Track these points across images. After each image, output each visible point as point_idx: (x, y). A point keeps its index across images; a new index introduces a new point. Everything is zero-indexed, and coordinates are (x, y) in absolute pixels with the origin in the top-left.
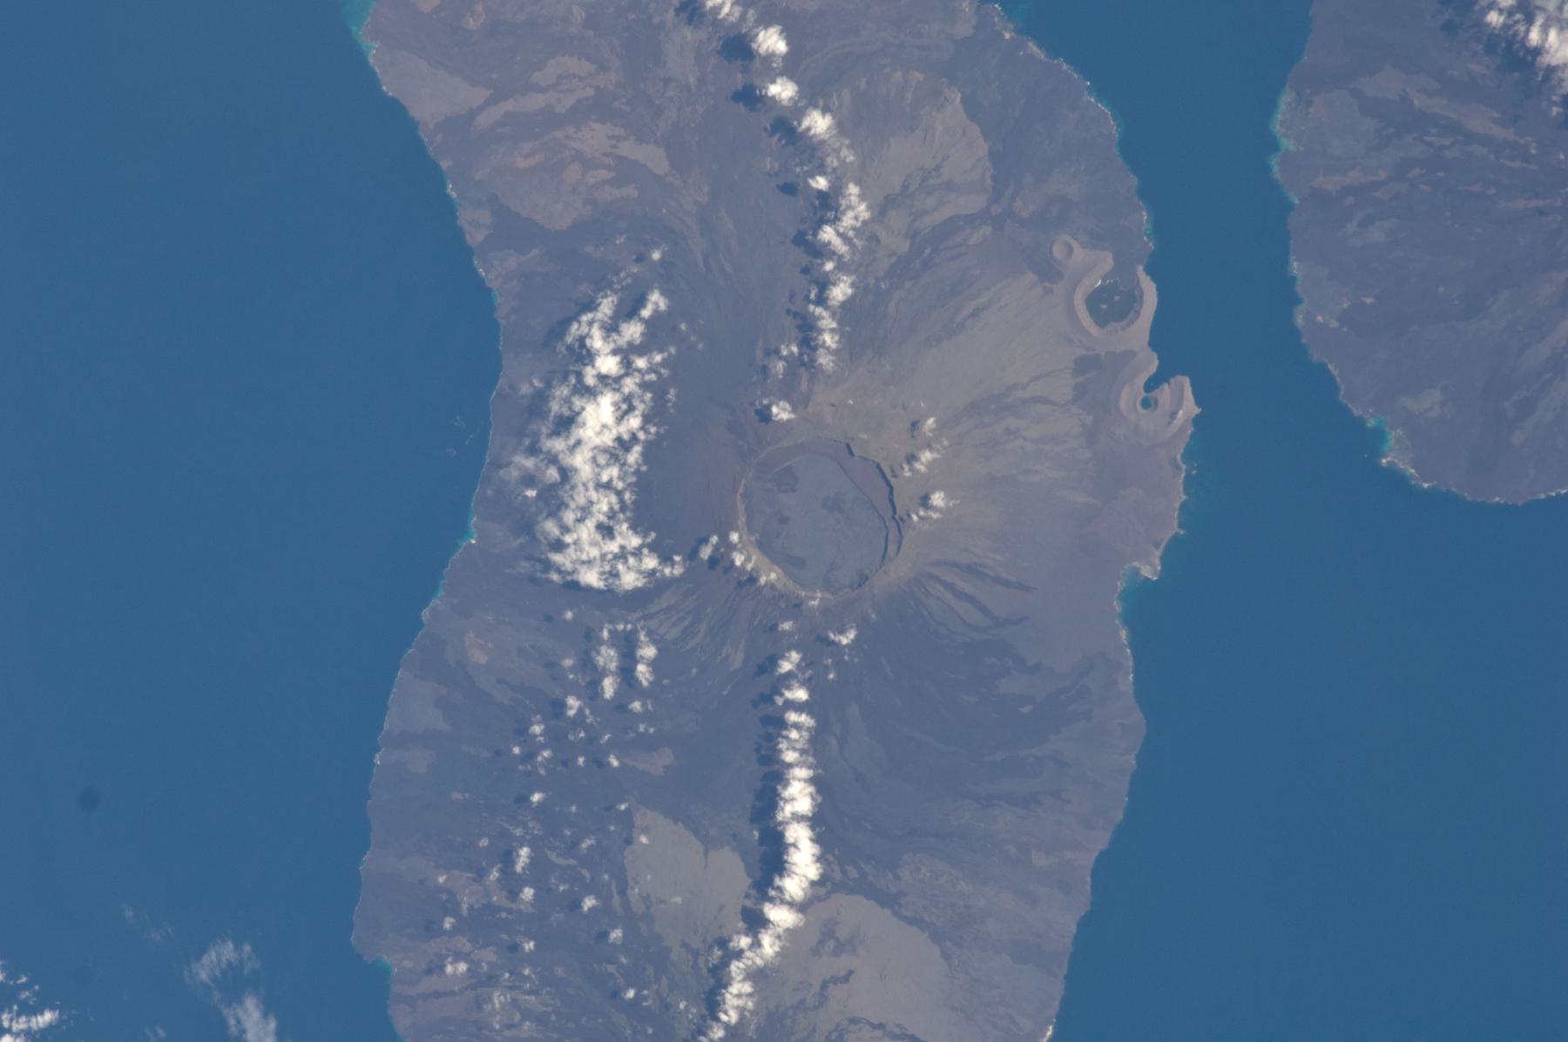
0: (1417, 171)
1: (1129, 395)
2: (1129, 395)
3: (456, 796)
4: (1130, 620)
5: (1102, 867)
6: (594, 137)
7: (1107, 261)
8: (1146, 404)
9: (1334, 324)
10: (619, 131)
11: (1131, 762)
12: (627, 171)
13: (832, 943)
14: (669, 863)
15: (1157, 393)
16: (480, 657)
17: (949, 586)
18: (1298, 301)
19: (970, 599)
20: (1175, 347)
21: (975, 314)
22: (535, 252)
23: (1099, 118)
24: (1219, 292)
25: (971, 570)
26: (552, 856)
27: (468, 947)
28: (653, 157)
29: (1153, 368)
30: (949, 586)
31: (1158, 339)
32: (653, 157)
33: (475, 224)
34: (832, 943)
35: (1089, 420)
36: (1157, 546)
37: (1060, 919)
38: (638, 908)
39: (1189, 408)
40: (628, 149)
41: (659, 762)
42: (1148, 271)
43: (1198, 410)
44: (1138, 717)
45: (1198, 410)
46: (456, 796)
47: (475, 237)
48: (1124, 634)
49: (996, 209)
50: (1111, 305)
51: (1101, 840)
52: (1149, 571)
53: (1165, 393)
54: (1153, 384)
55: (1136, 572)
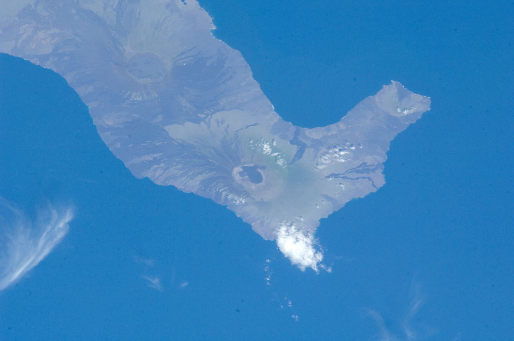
3: (130, 146)
4: (219, 38)
5: (255, 77)
6: (41, 34)
11: (242, 58)
13: (220, 123)
16: (110, 123)
17: (182, 59)
22: (51, 58)
25: (182, 53)
26: (157, 144)
27: (157, 166)
30: (182, 59)
33: (36, 61)
34: (220, 123)
37: (256, 89)
38: (181, 142)
40: (49, 32)
41: (160, 118)
44: (237, 51)
46: (130, 146)
47: (38, 63)
48: (220, 41)
51: (251, 74)
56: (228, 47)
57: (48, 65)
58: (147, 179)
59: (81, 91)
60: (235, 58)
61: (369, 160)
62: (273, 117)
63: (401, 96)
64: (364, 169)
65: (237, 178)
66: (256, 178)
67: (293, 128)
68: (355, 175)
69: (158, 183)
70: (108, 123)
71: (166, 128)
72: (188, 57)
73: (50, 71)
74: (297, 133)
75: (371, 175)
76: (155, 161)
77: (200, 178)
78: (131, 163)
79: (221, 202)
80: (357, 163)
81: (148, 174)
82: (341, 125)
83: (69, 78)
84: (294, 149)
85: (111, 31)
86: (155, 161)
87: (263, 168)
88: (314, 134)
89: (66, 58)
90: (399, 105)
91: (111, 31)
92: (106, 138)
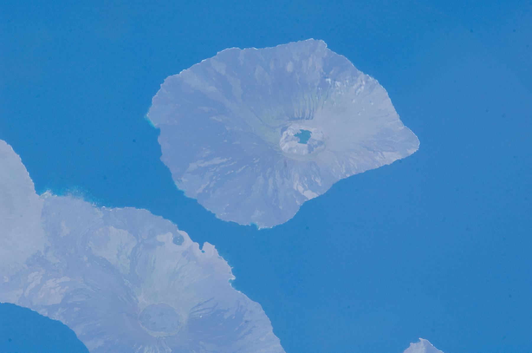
0: (214, 178)
1: (198, 252)
4: (238, 289)
6: (50, 283)
7: (171, 234)
8: (203, 252)
9: (225, 213)
10: (54, 279)
11: (263, 312)
15: (203, 249)
17: (198, 311)
18: (214, 214)
19: (204, 309)
20: (199, 238)
21: (154, 263)
22: (60, 309)
23: (143, 213)
24: (198, 223)
25: (199, 305)
29: (198, 245)
30: (198, 311)
31: (194, 239)
33: (44, 312)
35: (195, 262)
36: (230, 273)
39: (213, 247)
42: (180, 229)
43: (214, 246)
44: (257, 304)
45: (214, 246)
47: (46, 314)
48: (239, 292)
49: (140, 241)
50: (178, 241)
52: (233, 278)
53: (204, 248)
54: (201, 248)
55: (231, 280)
56: (248, 299)
57: (56, 316)
60: (255, 311)
72: (204, 309)
85: (125, 280)
89: (76, 309)
91: (125, 280)
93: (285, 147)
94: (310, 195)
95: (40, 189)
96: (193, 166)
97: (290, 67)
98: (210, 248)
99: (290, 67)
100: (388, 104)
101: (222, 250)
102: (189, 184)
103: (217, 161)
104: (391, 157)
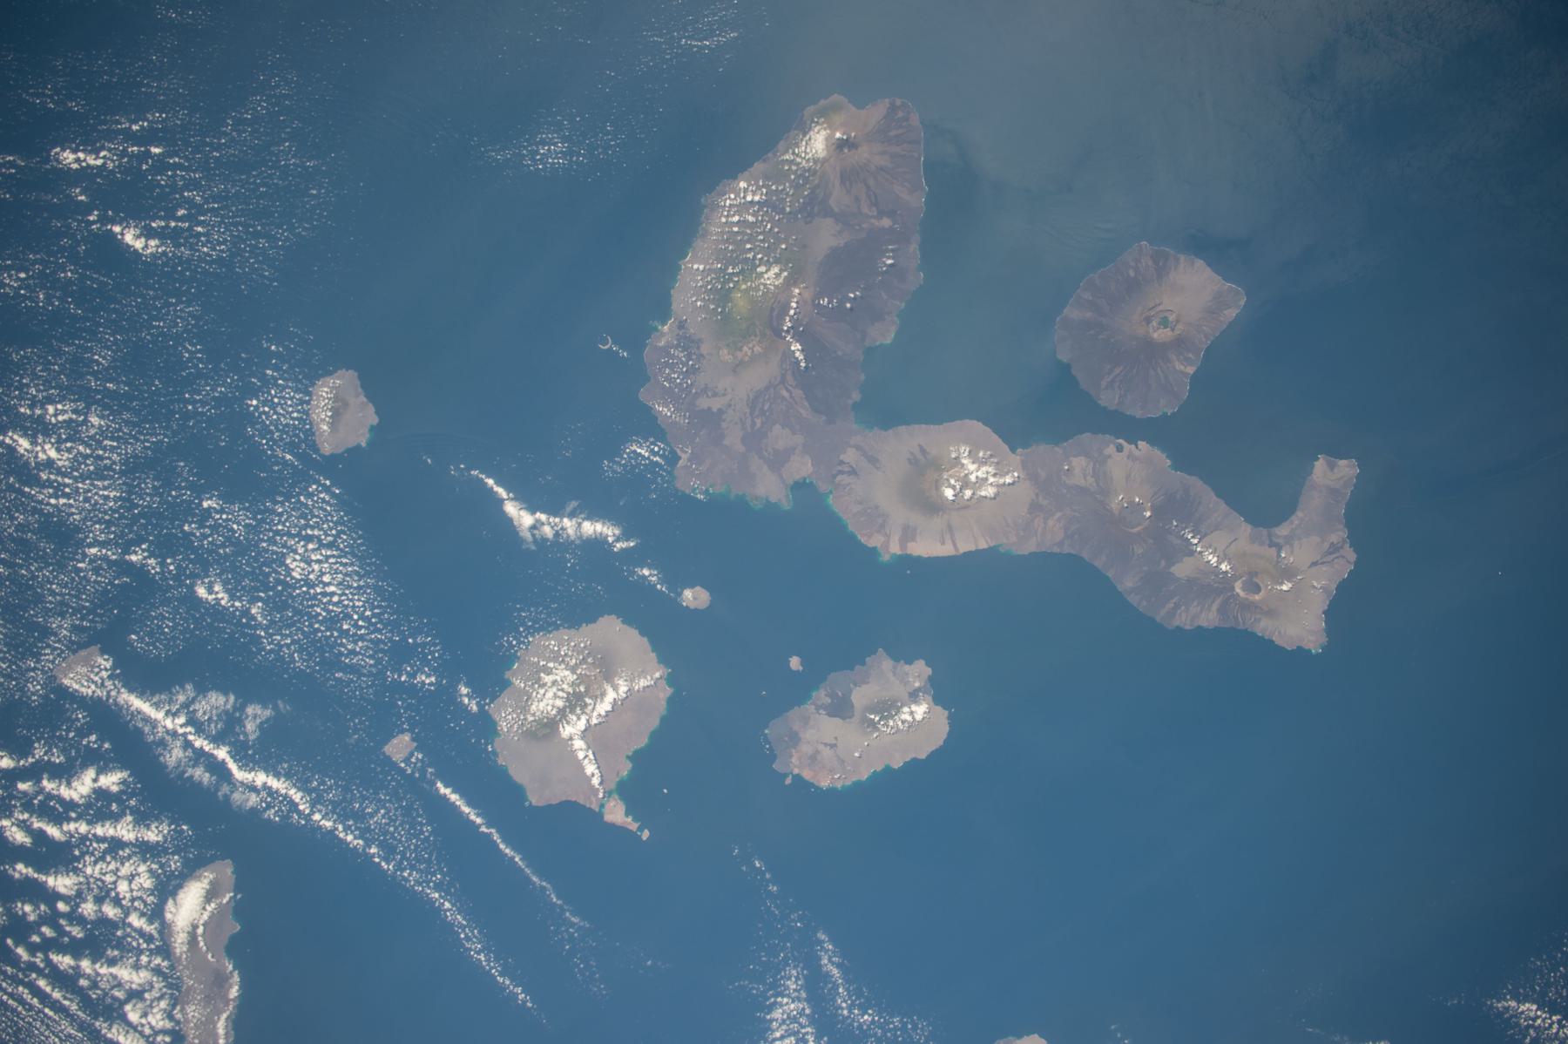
1: (1136, 452)
2: (1136, 452)
6: (1051, 522)
12: (1059, 520)
14: (1182, 569)
23: (1086, 436)
28: (1058, 514)
32: (1058, 514)
33: (1056, 550)
37: (1223, 506)
41: (1163, 563)
50: (1120, 449)
57: (1066, 549)
58: (1178, 628)
59: (1099, 563)
60: (1195, 483)
61: (1334, 538)
62: (1246, 529)
63: (1332, 466)
64: (1334, 548)
65: (1242, 594)
66: (1258, 589)
67: (1264, 532)
68: (1329, 558)
69: (1188, 627)
70: (1128, 583)
71: (1172, 569)
73: (1069, 555)
74: (1270, 535)
75: (1342, 552)
76: (1177, 606)
77: (1215, 607)
78: (1160, 616)
79: (1241, 627)
80: (1326, 545)
81: (1176, 623)
82: (1299, 514)
83: (1085, 555)
84: (1273, 551)
86: (1177, 606)
87: (1256, 574)
88: (1283, 531)
90: (1332, 475)
92: (1133, 599)
93: (1155, 335)
94: (1191, 370)
95: (1013, 450)
96: (1104, 384)
97: (1132, 273)
98: (1141, 444)
99: (1132, 273)
100: (1208, 273)
101: (1152, 442)
102: (1108, 399)
103: (1117, 371)
104: (1231, 313)
